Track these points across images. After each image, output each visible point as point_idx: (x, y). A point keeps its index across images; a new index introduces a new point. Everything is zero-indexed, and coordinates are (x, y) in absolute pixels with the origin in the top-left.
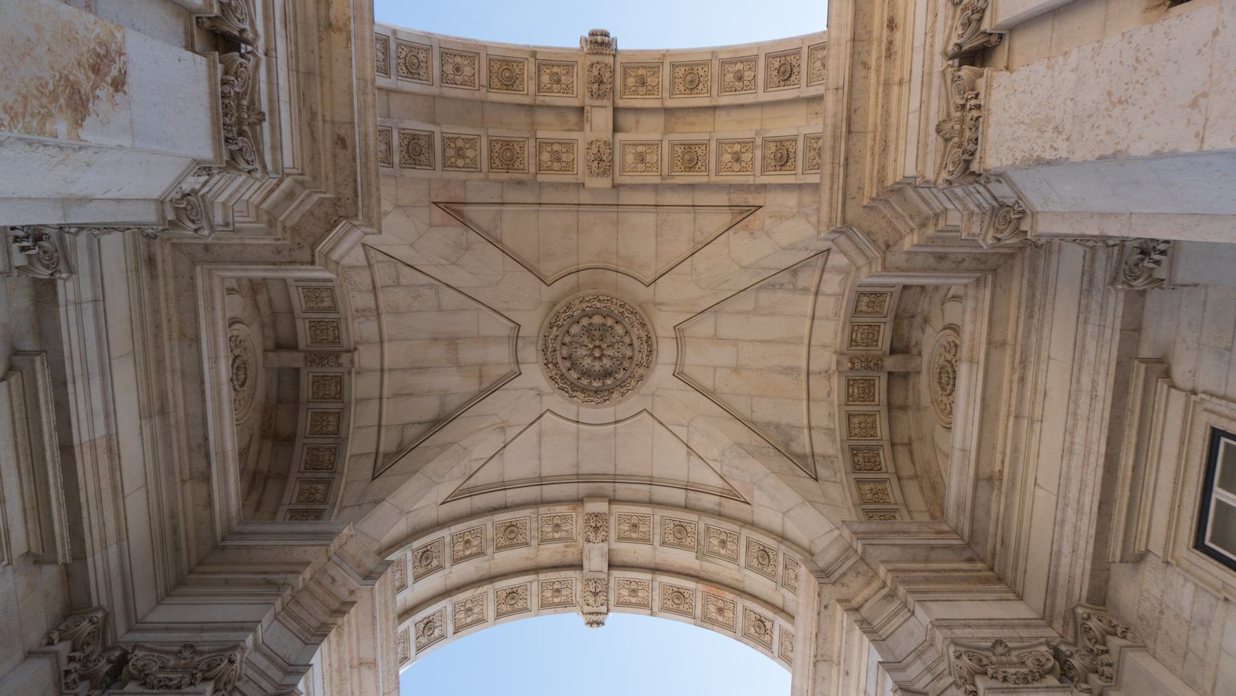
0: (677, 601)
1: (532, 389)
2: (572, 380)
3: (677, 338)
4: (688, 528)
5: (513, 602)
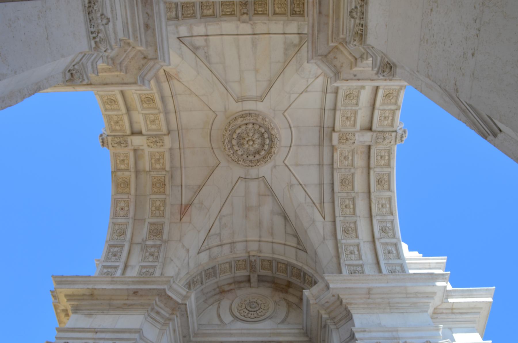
1: (272, 170)
3: (242, 101)
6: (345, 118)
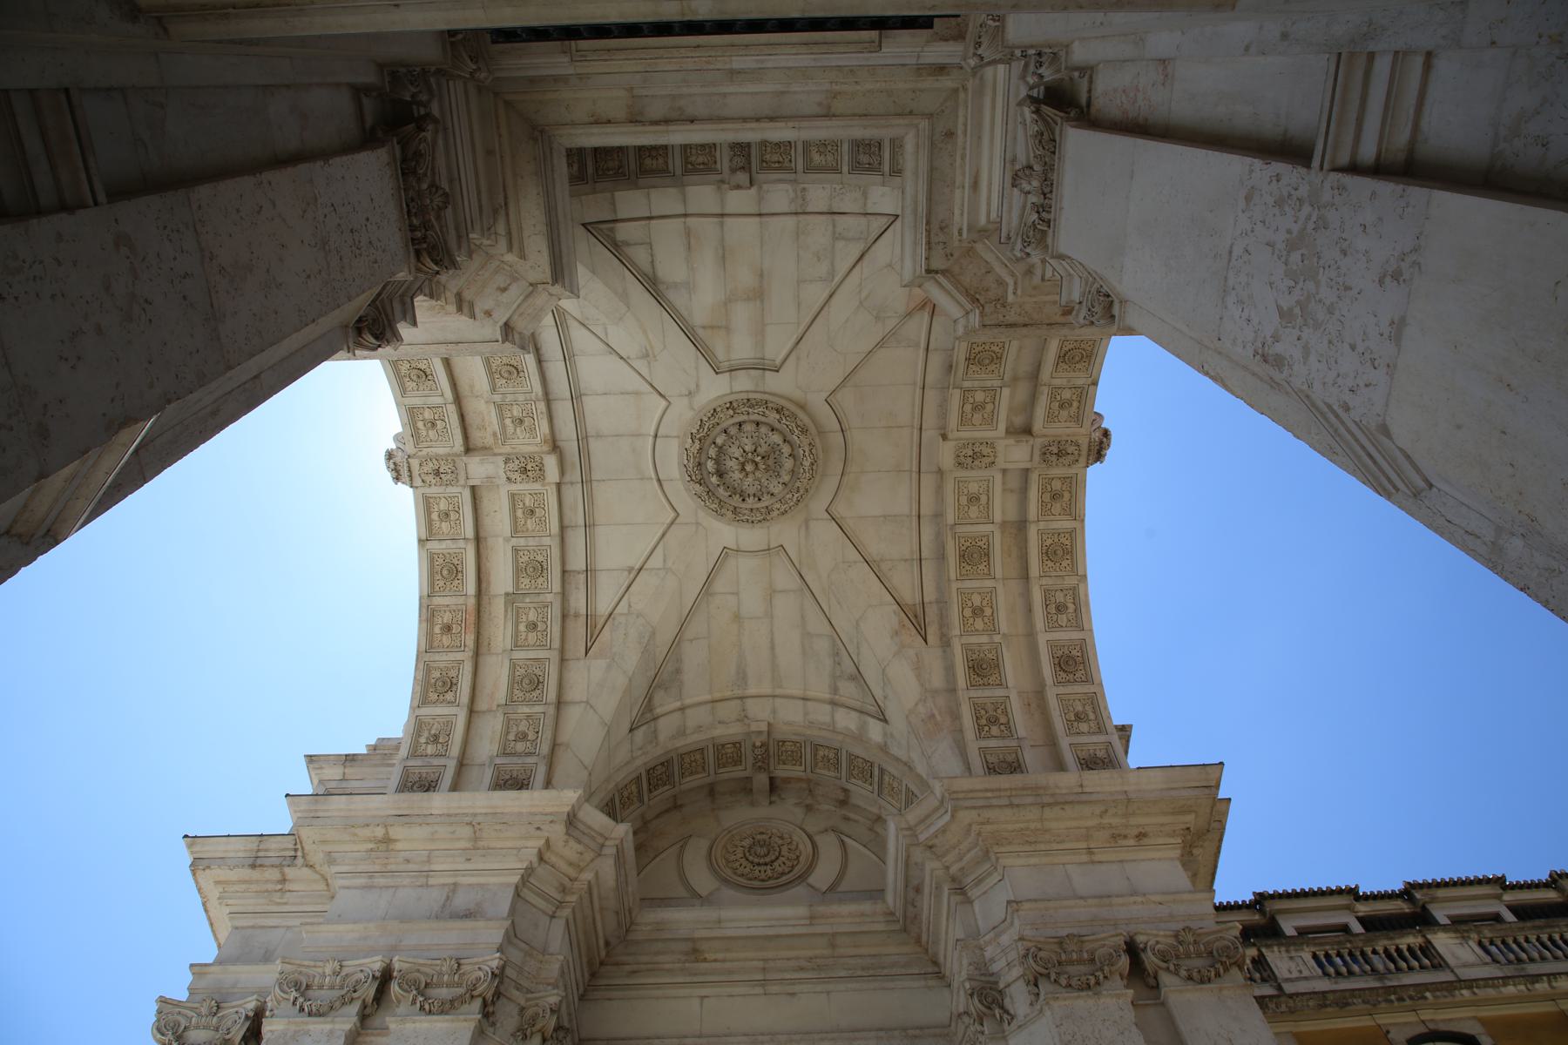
0: (445, 572)
1: (697, 386)
2: (712, 436)
3: (769, 550)
5: (415, 378)
6: (537, 515)
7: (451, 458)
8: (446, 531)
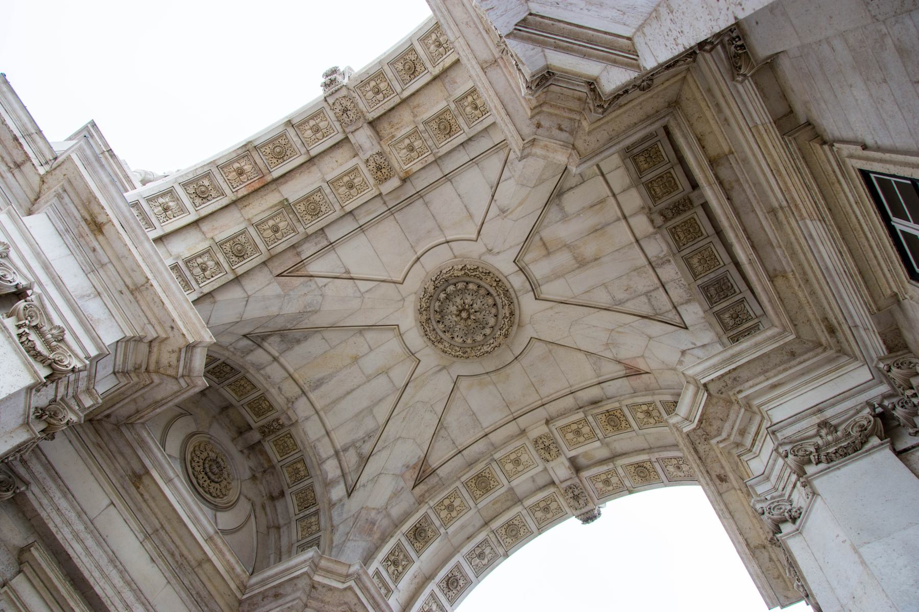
0: (278, 150)
3: (413, 354)
4: (309, 217)
6: (351, 191)
7: (361, 115)
8: (305, 135)
